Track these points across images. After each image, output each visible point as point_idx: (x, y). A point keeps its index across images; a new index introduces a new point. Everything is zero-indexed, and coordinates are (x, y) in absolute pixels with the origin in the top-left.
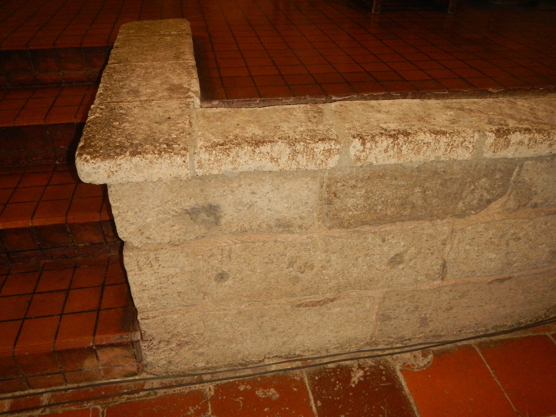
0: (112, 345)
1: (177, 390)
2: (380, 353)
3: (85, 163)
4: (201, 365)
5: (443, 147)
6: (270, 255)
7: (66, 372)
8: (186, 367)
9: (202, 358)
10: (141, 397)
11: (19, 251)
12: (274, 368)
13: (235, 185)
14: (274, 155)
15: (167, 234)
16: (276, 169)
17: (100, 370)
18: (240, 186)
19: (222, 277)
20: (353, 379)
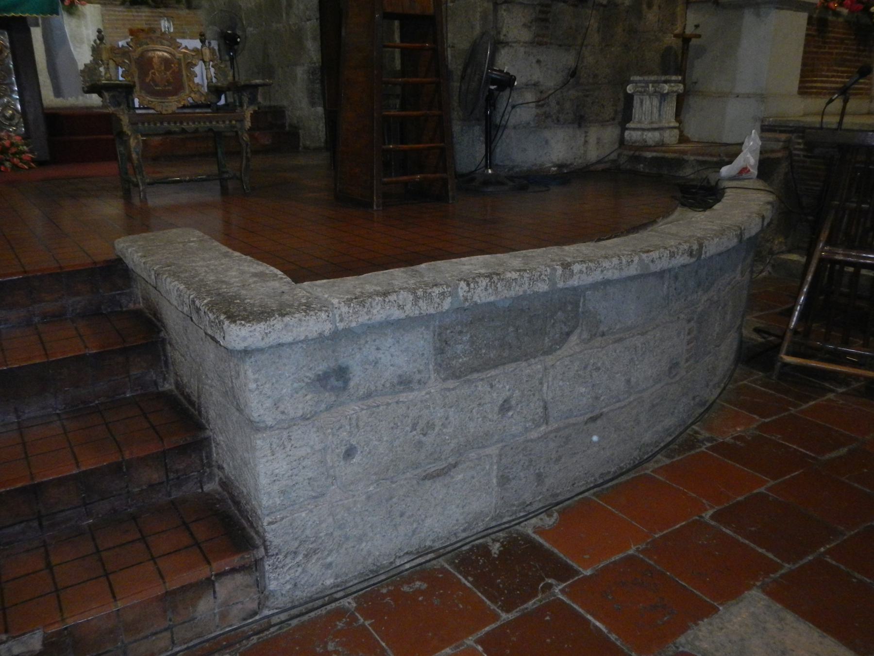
0: (233, 571)
1: (312, 614)
2: (507, 525)
3: (242, 328)
4: (329, 582)
5: (527, 282)
6: (394, 418)
8: (314, 589)
9: (330, 571)
10: (274, 632)
12: (407, 566)
13: (362, 342)
14: (401, 303)
15: (300, 406)
16: (403, 316)
17: (215, 615)
18: (367, 342)
19: (349, 453)
20: (493, 551)
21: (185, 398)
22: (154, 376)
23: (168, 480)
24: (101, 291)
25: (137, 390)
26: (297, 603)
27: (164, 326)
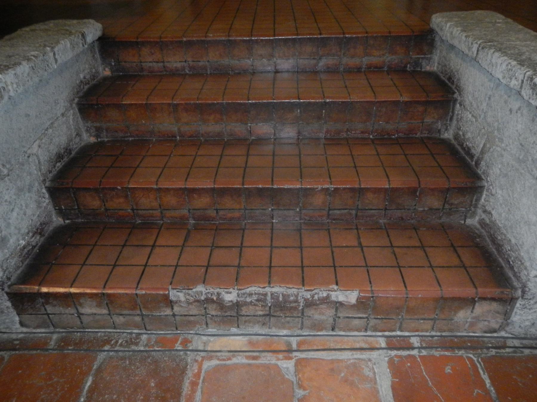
7: (438, 319)
10: (509, 353)
11: (367, 210)
17: (467, 322)
21: (464, 149)
22: (440, 126)
23: (443, 209)
24: (411, 53)
25: (425, 133)
26: (529, 336)
27: (459, 89)
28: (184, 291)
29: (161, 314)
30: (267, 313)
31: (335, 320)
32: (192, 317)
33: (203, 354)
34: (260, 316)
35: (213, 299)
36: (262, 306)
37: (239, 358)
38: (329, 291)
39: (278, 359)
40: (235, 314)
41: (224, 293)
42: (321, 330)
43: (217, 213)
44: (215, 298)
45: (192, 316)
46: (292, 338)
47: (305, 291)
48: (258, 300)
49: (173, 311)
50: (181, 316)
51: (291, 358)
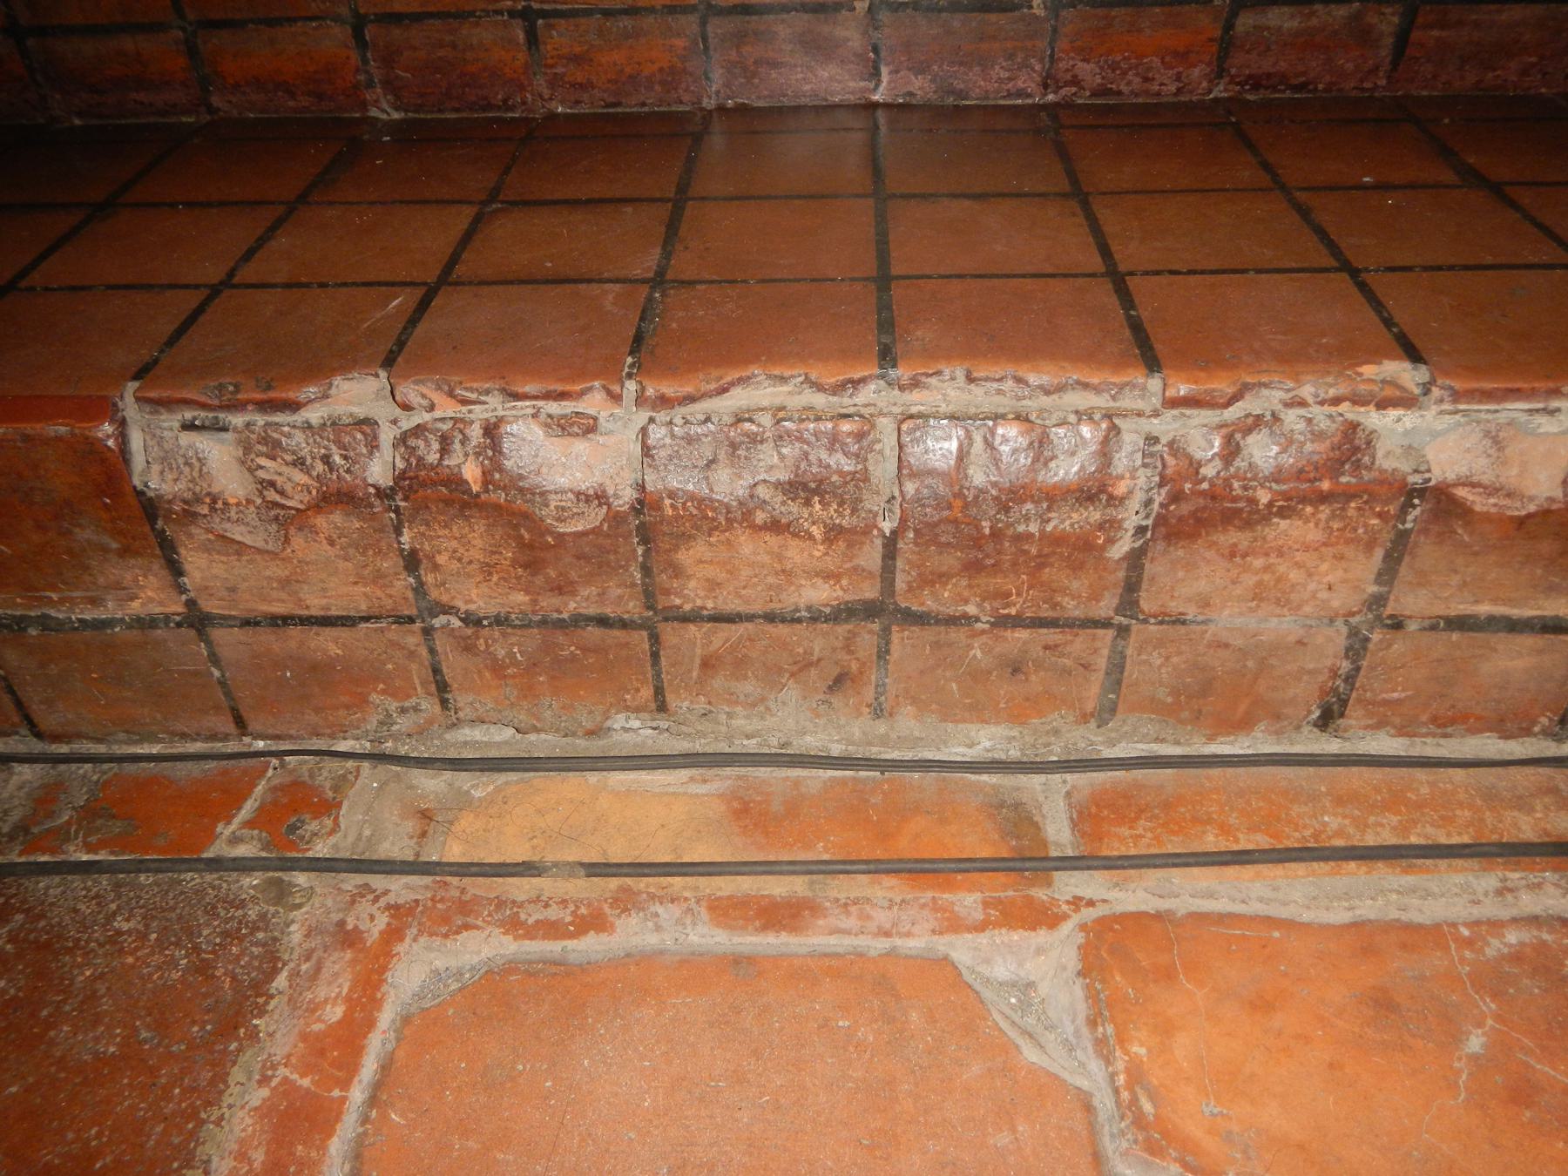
28: (237, 420)
29: (101, 614)
30: (870, 592)
31: (1357, 647)
32: (328, 632)
33: (400, 888)
34: (816, 617)
35: (455, 482)
36: (834, 533)
37: (667, 913)
38: (1358, 400)
39: (954, 924)
40: (633, 608)
41: (537, 432)
42: (1244, 725)
43: (533, 39)
44: (471, 472)
45: (326, 621)
46: (1037, 780)
47: (1173, 403)
48: (801, 488)
49: (182, 590)
50: (247, 623)
51: (1046, 917)
